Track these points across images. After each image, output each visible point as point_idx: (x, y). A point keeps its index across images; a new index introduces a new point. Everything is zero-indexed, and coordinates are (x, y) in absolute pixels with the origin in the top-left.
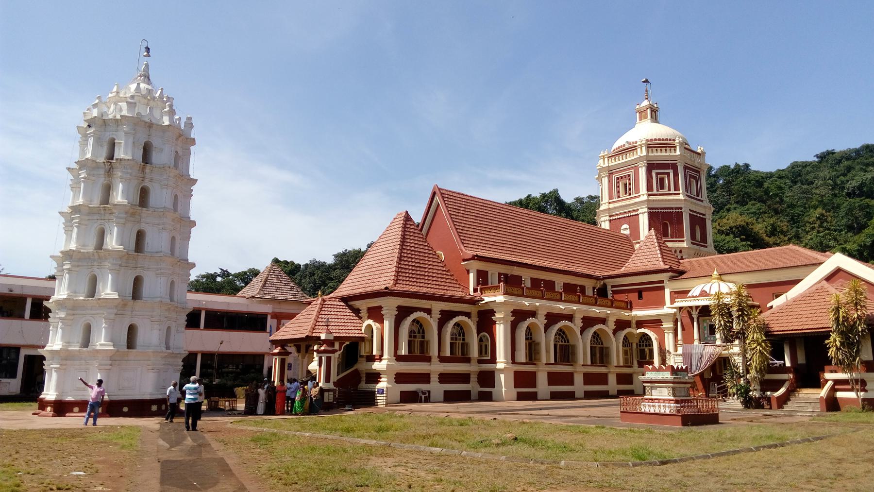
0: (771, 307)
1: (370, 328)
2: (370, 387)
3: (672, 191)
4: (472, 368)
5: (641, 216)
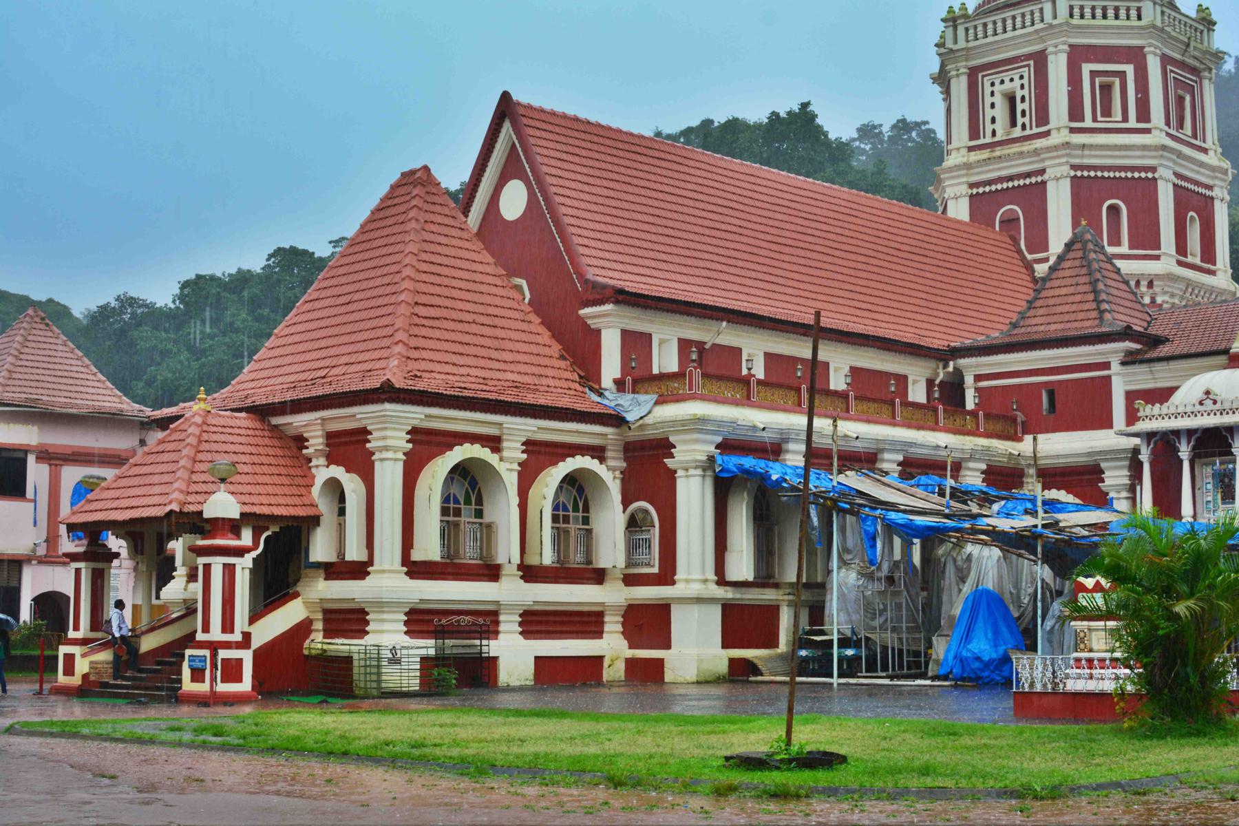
1: (334, 487)
2: (341, 646)
3: (1132, 123)
4: (611, 596)
5: (1051, 187)
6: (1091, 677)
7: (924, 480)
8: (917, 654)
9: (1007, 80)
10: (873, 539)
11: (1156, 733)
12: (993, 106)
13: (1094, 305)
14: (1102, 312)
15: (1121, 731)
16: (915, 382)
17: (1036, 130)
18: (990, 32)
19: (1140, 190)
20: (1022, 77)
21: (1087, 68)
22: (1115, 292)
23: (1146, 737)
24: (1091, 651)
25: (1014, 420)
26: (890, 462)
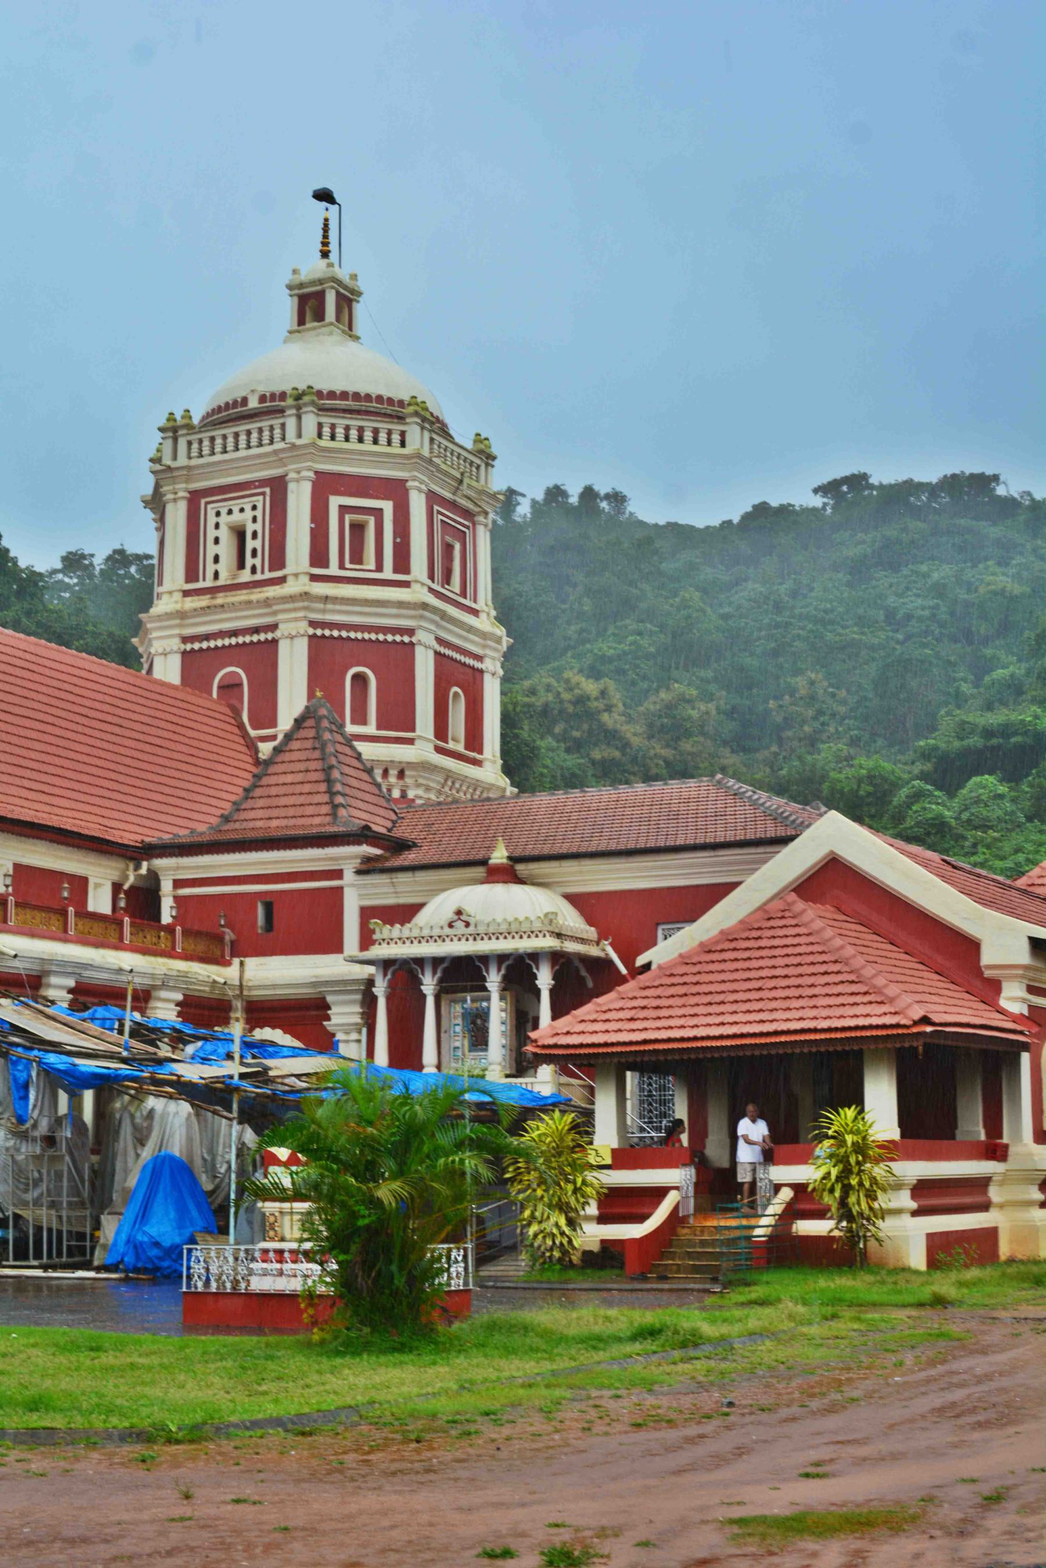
0: (647, 967)
3: (388, 574)
5: (283, 647)
6: (281, 1273)
7: (101, 1012)
8: (81, 1236)
9: (236, 510)
10: (26, 1087)
11: (352, 1348)
12: (217, 541)
13: (326, 798)
14: (336, 807)
15: (309, 1345)
16: (97, 886)
17: (268, 575)
18: (218, 448)
19: (394, 658)
20: (254, 508)
21: (335, 502)
22: (354, 783)
23: (338, 1353)
24: (283, 1239)
25: (219, 939)
26: (58, 989)
